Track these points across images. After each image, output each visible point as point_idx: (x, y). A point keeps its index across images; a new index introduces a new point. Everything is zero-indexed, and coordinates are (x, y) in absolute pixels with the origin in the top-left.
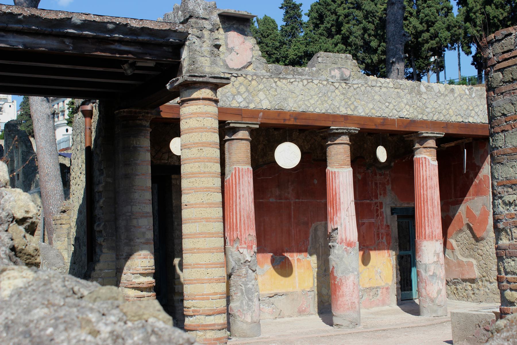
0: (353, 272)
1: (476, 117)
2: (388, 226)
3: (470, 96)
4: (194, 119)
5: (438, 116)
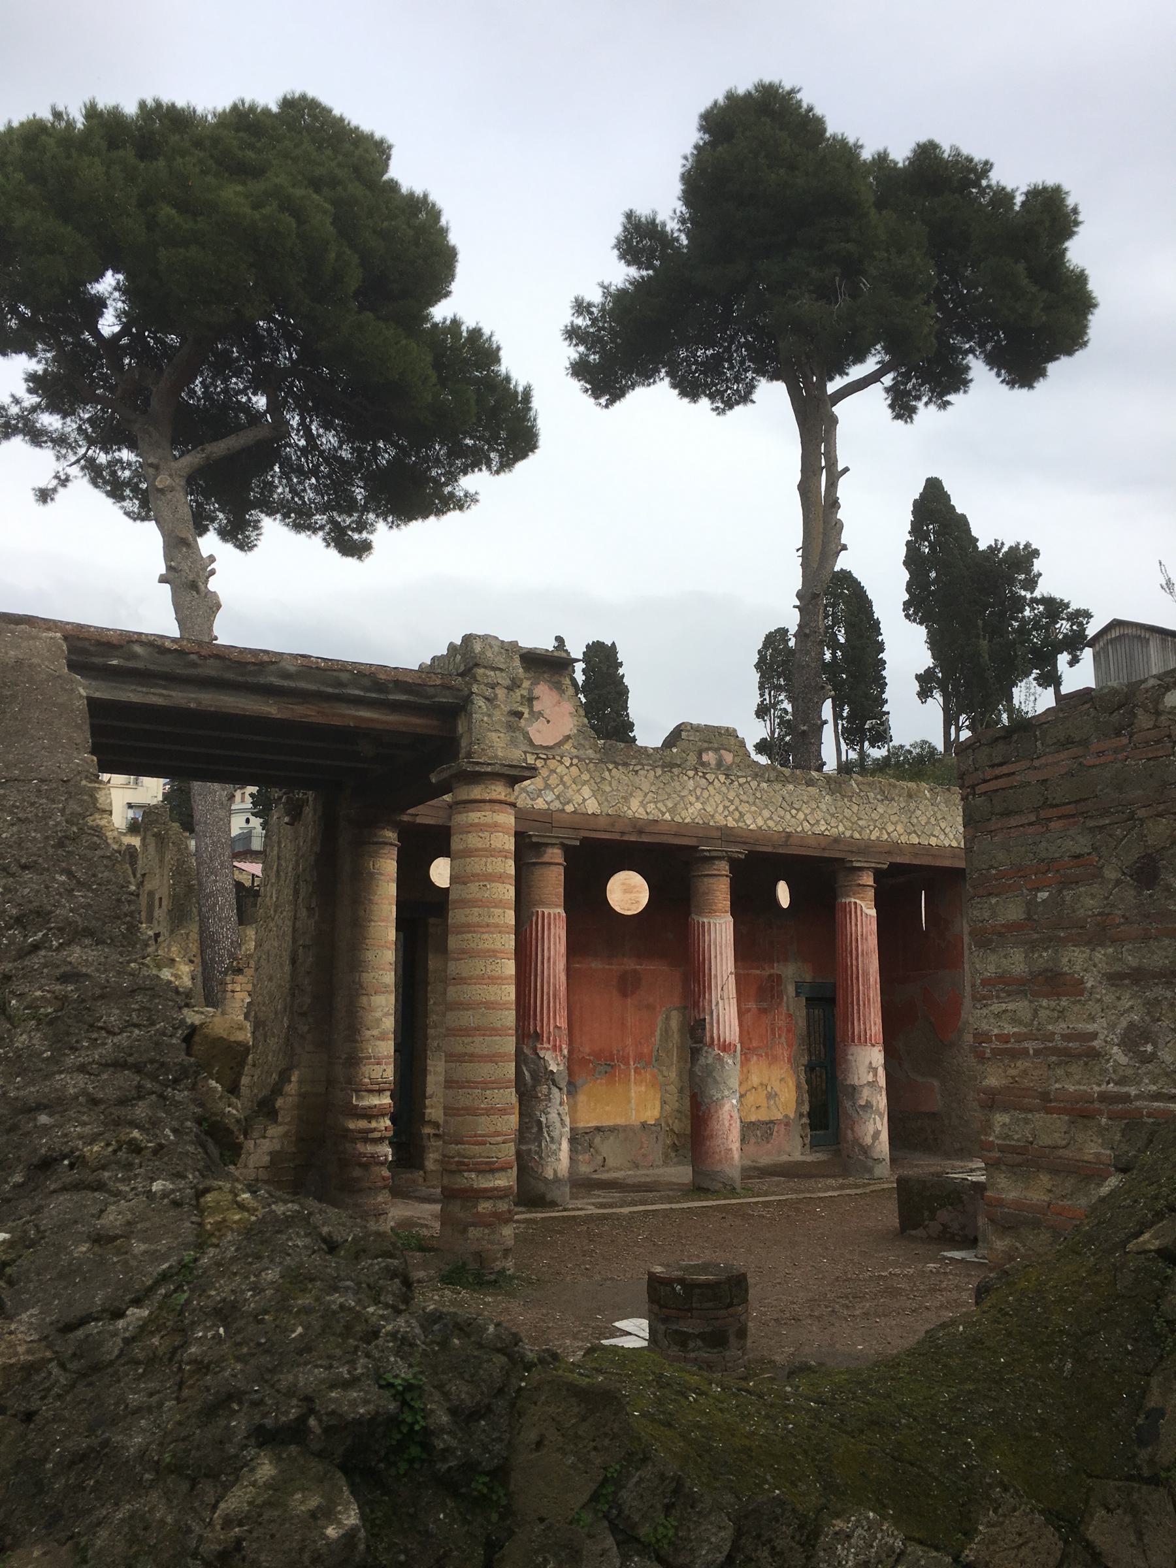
1: (942, 837)
5: (878, 834)
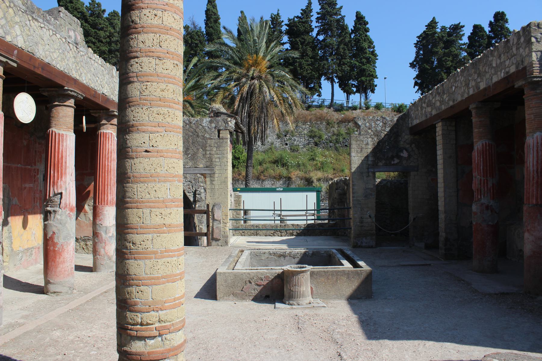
4: (170, 14)
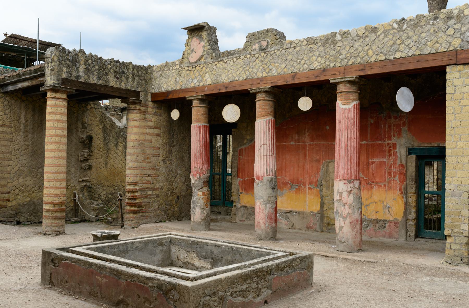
0: (259, 199)
1: (406, 51)
2: (402, 166)
3: (399, 29)
5: (353, 61)
